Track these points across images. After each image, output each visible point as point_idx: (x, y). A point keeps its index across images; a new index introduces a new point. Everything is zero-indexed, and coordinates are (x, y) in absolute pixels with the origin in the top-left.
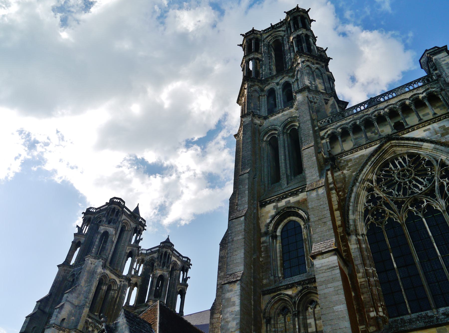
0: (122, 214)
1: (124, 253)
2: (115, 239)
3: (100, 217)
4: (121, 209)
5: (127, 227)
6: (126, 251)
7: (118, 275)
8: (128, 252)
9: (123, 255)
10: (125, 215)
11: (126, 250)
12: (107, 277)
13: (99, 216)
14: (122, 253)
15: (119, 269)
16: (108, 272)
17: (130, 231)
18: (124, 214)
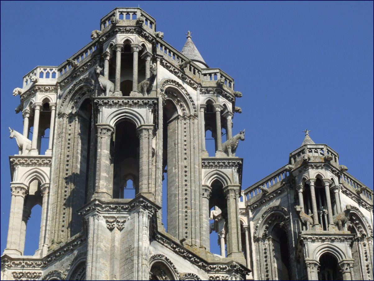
0: (154, 60)
1: (197, 189)
2: (156, 143)
3: (81, 88)
4: (149, 46)
5: (181, 106)
6: (203, 183)
7: (202, 260)
8: (209, 184)
9: (198, 194)
10: (167, 67)
11: (200, 180)
12: (170, 272)
13: (77, 88)
14: (189, 189)
15: (198, 241)
16: (168, 253)
17: (196, 116)
18: (162, 63)
